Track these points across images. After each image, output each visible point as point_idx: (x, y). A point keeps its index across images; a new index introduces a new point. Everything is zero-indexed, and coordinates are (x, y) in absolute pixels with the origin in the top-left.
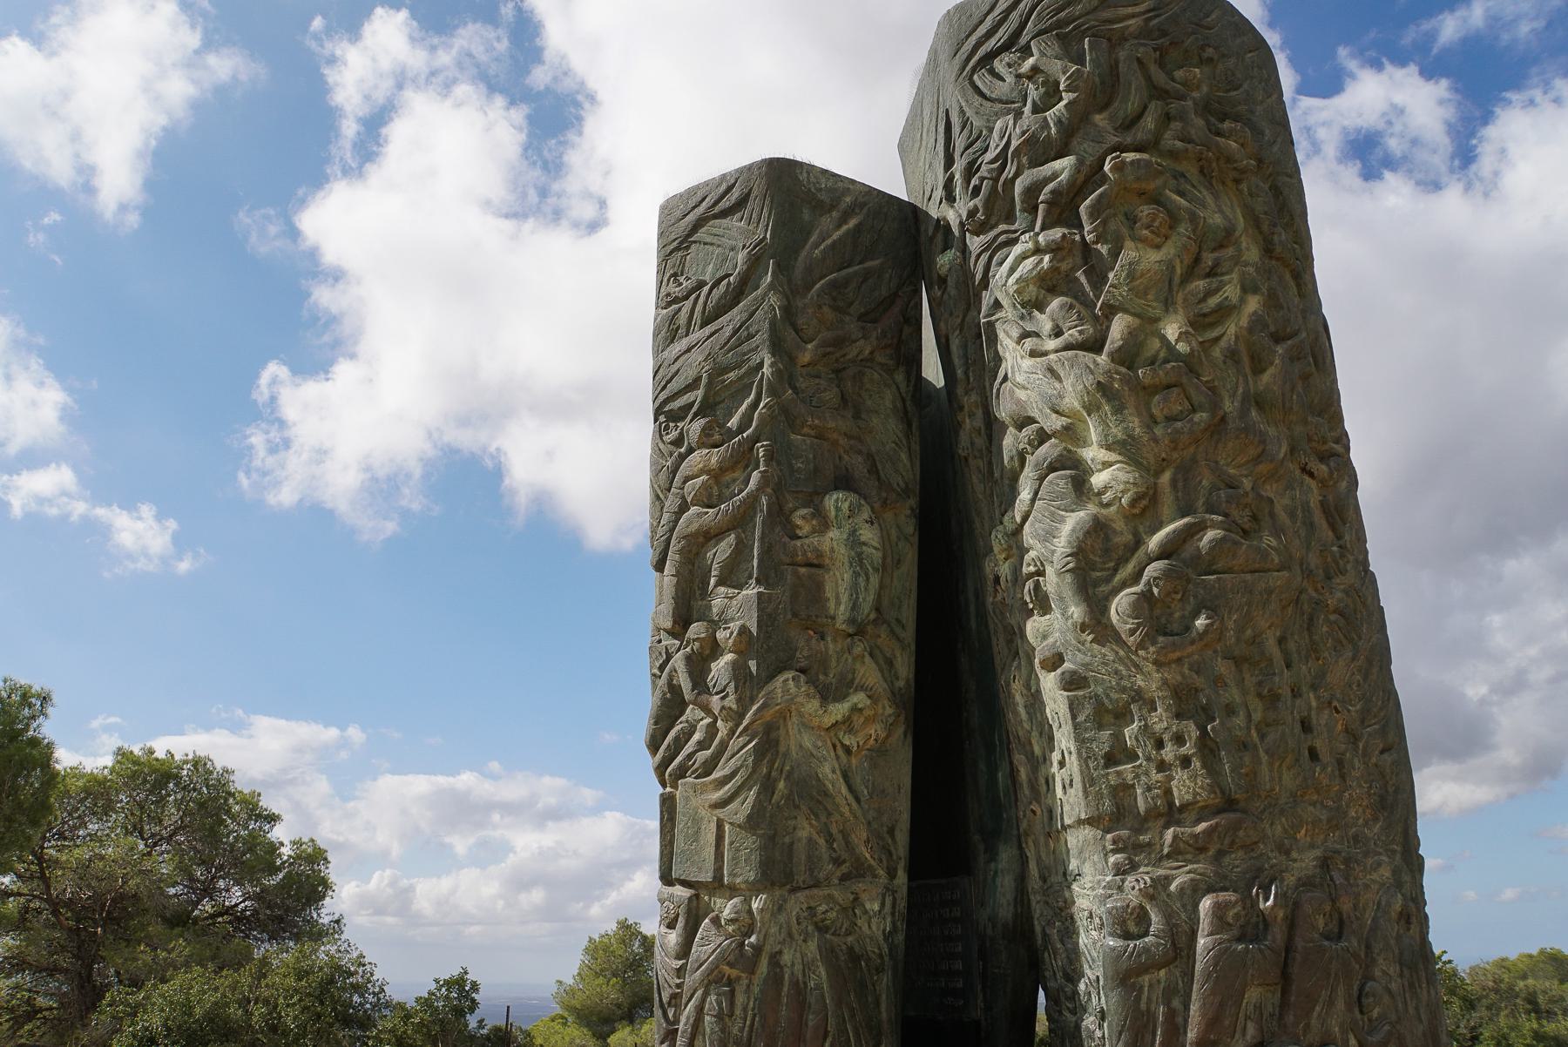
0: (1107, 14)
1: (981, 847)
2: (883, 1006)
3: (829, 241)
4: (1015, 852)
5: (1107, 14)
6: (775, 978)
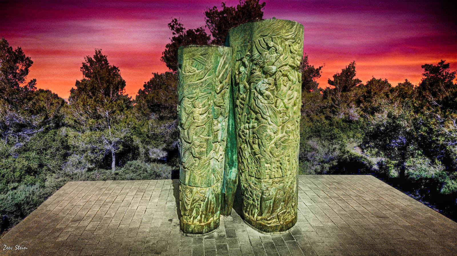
0: (286, 34)
1: (228, 167)
3: (222, 65)
4: (236, 170)
5: (286, 34)
6: (208, 201)
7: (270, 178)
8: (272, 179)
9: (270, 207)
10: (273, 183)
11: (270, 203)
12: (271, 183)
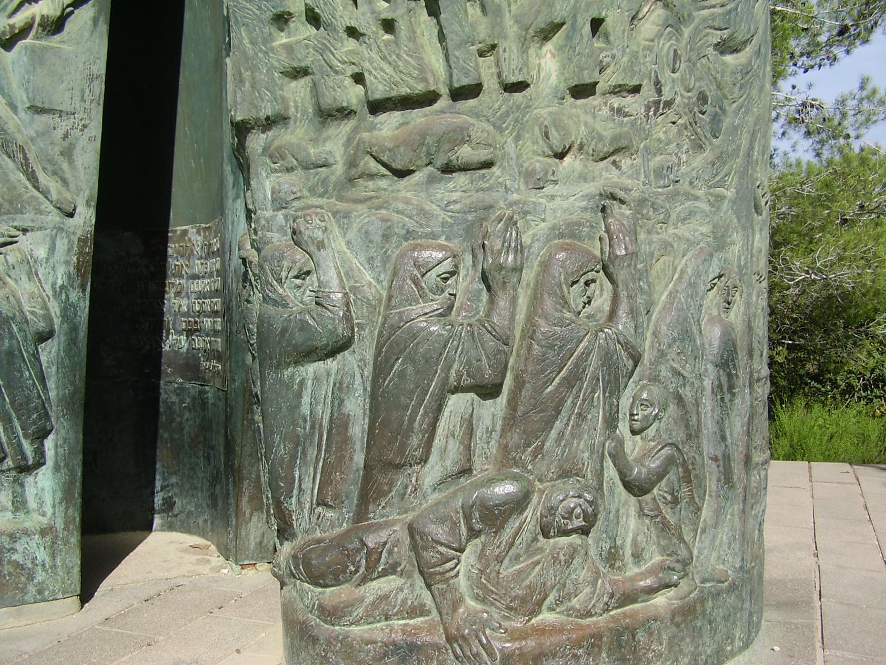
2: (51, 384)
7: (330, 114)
8: (347, 127)
9: (346, 440)
10: (352, 164)
11: (341, 389)
12: (339, 169)
